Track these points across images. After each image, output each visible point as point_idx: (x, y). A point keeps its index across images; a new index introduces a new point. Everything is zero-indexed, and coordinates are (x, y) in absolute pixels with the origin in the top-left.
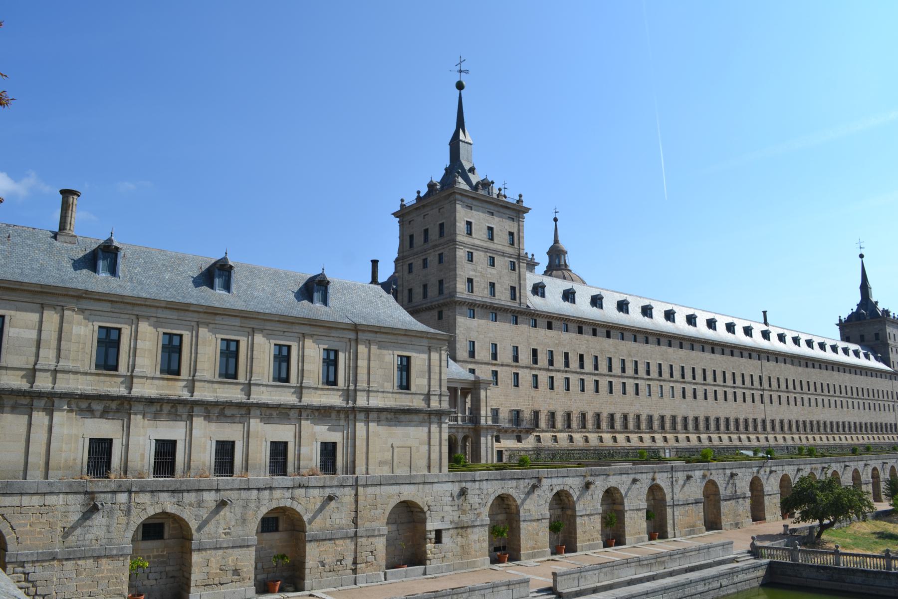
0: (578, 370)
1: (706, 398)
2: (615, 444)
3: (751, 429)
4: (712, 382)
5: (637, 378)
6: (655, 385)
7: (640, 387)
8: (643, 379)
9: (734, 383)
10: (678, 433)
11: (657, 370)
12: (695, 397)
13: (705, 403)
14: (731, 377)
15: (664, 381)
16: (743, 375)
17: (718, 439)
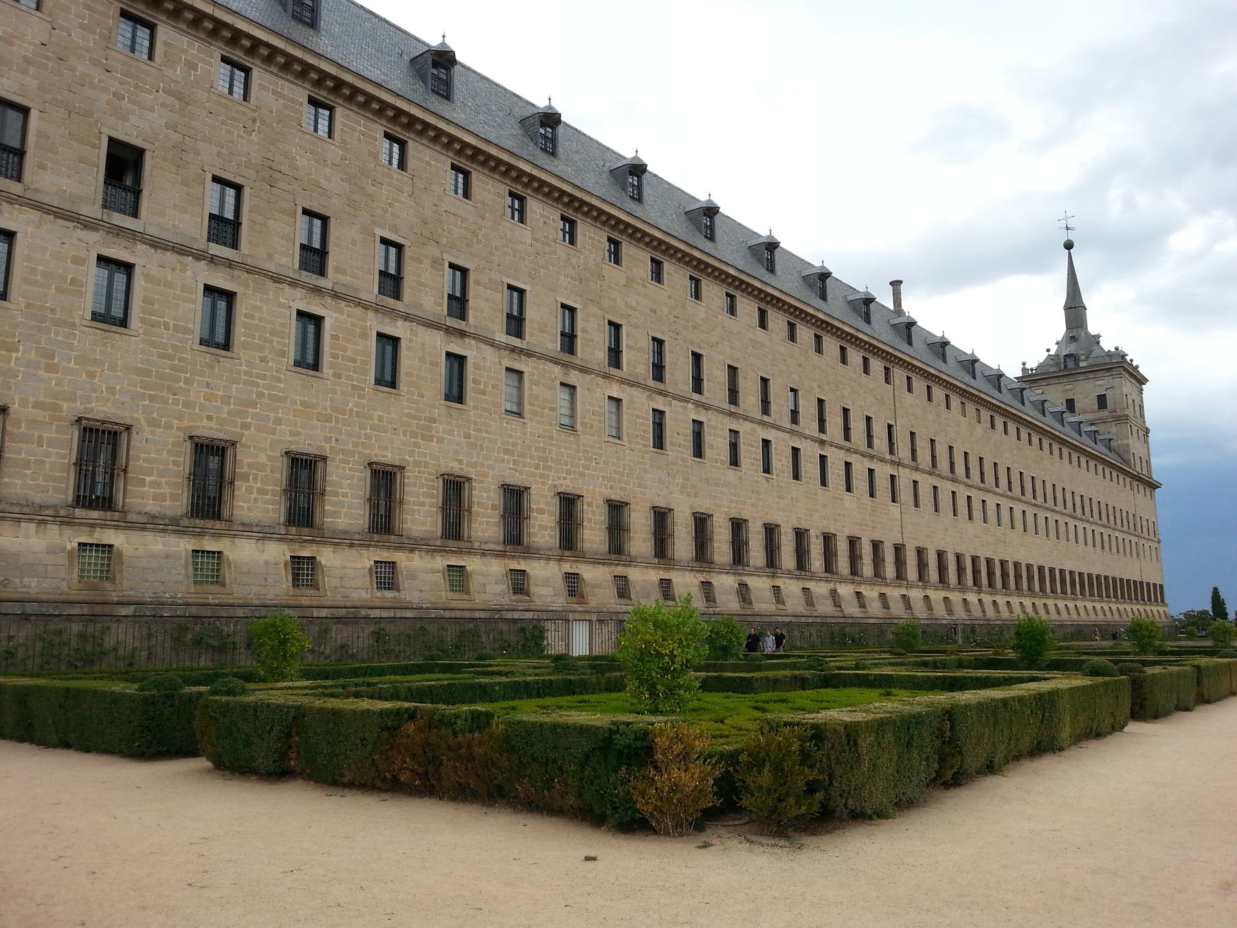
0: (92, 210)
1: (735, 462)
2: (306, 597)
3: (867, 569)
4: (756, 413)
5: (462, 334)
6: (542, 380)
7: (470, 372)
8: (492, 344)
9: (822, 429)
10: (631, 561)
11: (556, 324)
12: (698, 451)
13: (731, 475)
14: (814, 410)
15: (584, 370)
16: (846, 411)
17: (769, 594)
